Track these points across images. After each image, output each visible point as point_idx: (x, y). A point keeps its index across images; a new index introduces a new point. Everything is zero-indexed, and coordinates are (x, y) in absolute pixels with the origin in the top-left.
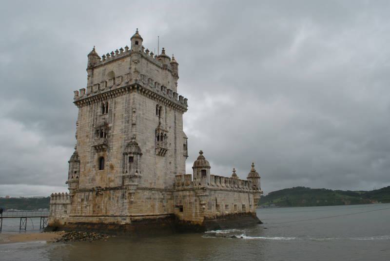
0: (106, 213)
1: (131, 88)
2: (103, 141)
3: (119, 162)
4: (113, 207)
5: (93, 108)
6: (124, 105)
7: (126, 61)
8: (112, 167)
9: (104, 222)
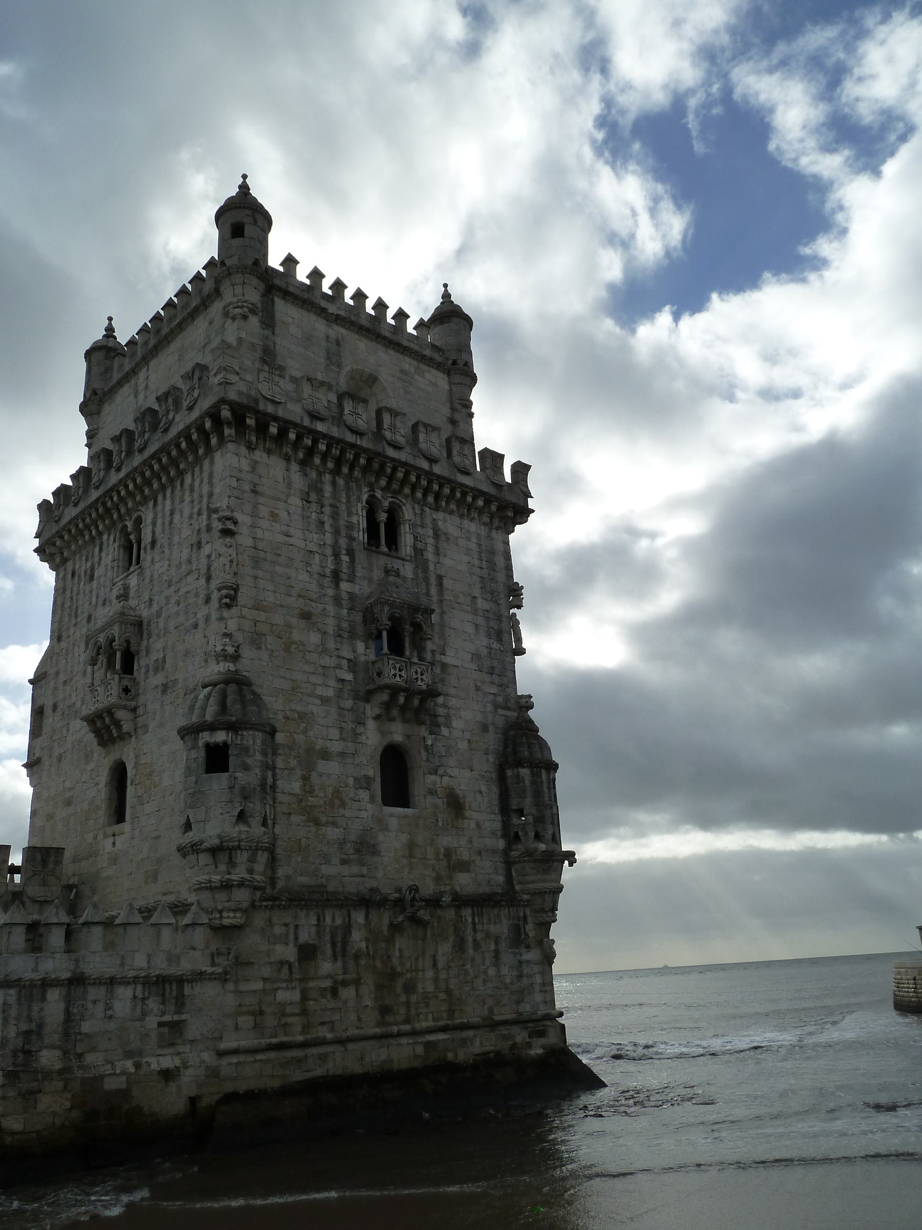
0: (451, 1013)
2: (427, 678)
3: (484, 789)
4: (479, 982)
5: (327, 494)
6: (476, 562)
7: (428, 375)
8: (456, 804)
9: (450, 1056)
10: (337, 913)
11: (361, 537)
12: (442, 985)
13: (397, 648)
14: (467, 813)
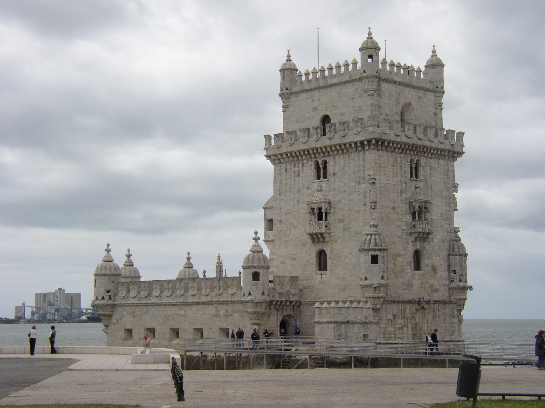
1: (456, 155)
7: (427, 96)
8: (434, 269)
10: (403, 305)
11: (408, 175)
12: (429, 329)
13: (420, 218)
14: (437, 272)
